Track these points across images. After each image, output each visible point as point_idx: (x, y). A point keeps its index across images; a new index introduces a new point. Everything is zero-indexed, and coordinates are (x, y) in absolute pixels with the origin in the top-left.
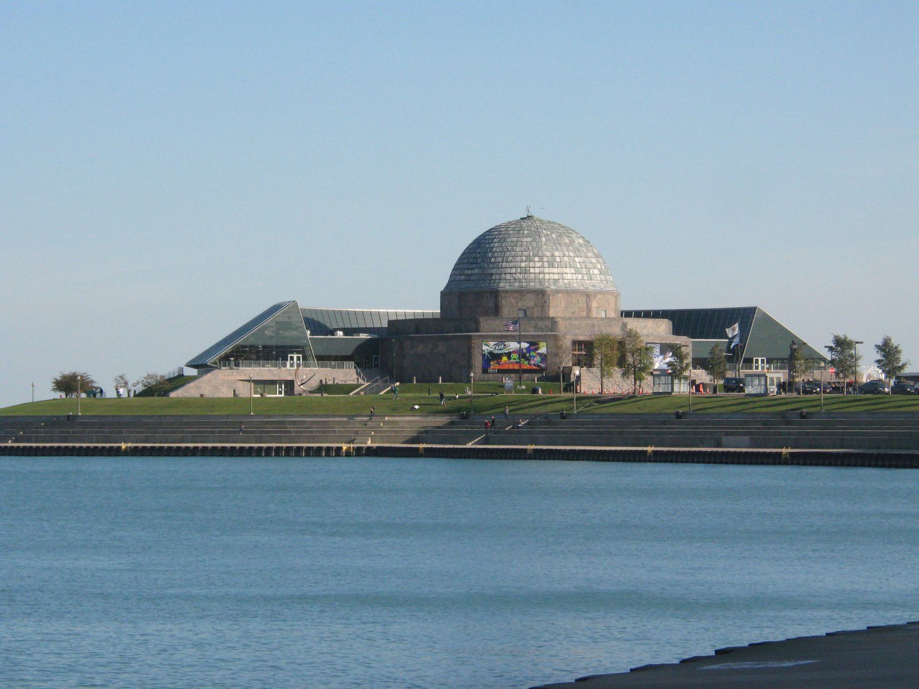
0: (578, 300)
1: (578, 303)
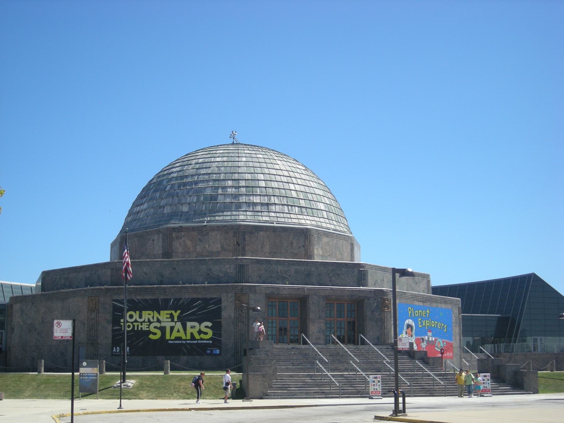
0: (292, 243)
1: (292, 246)
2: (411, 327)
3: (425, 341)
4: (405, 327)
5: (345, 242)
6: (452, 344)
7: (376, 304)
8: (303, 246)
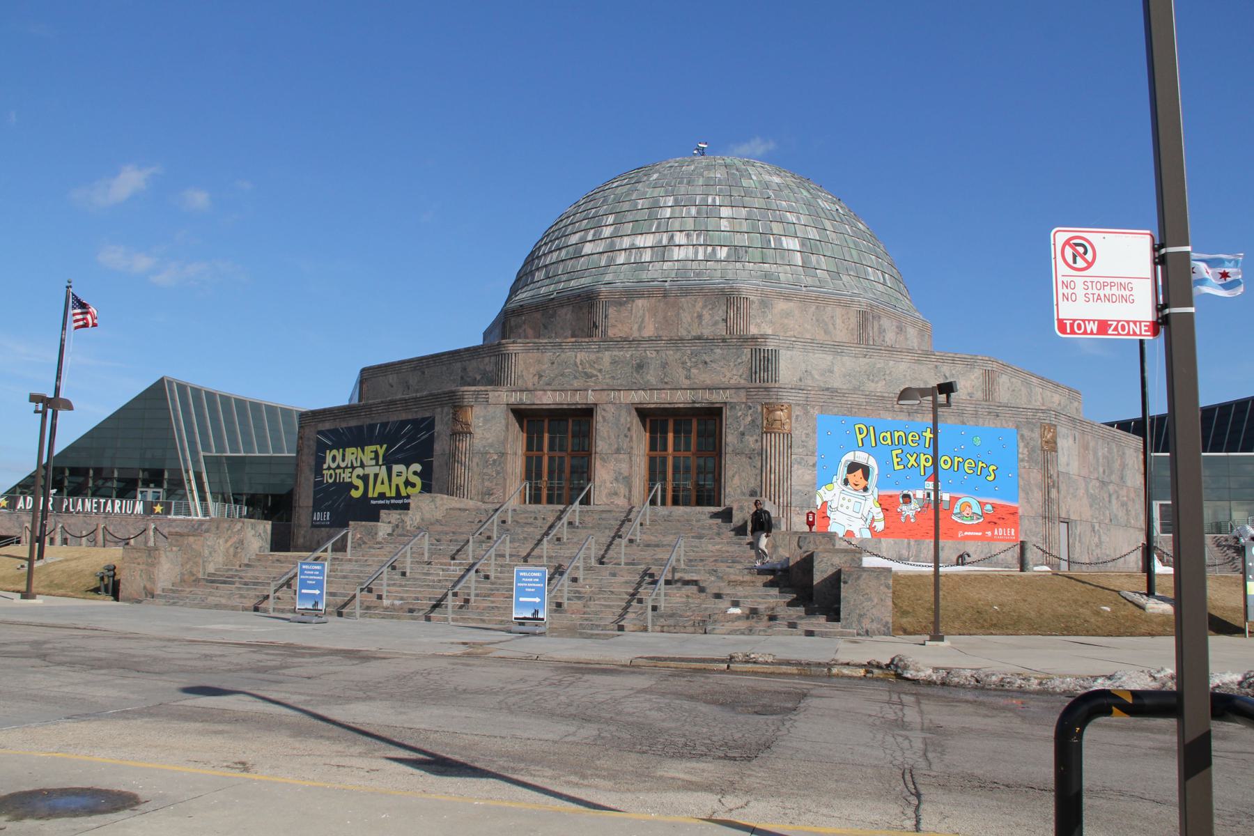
0: (700, 317)
1: (700, 324)
3: (913, 500)
4: (842, 471)
5: (839, 311)
6: (1017, 508)
7: (750, 418)
8: (723, 320)
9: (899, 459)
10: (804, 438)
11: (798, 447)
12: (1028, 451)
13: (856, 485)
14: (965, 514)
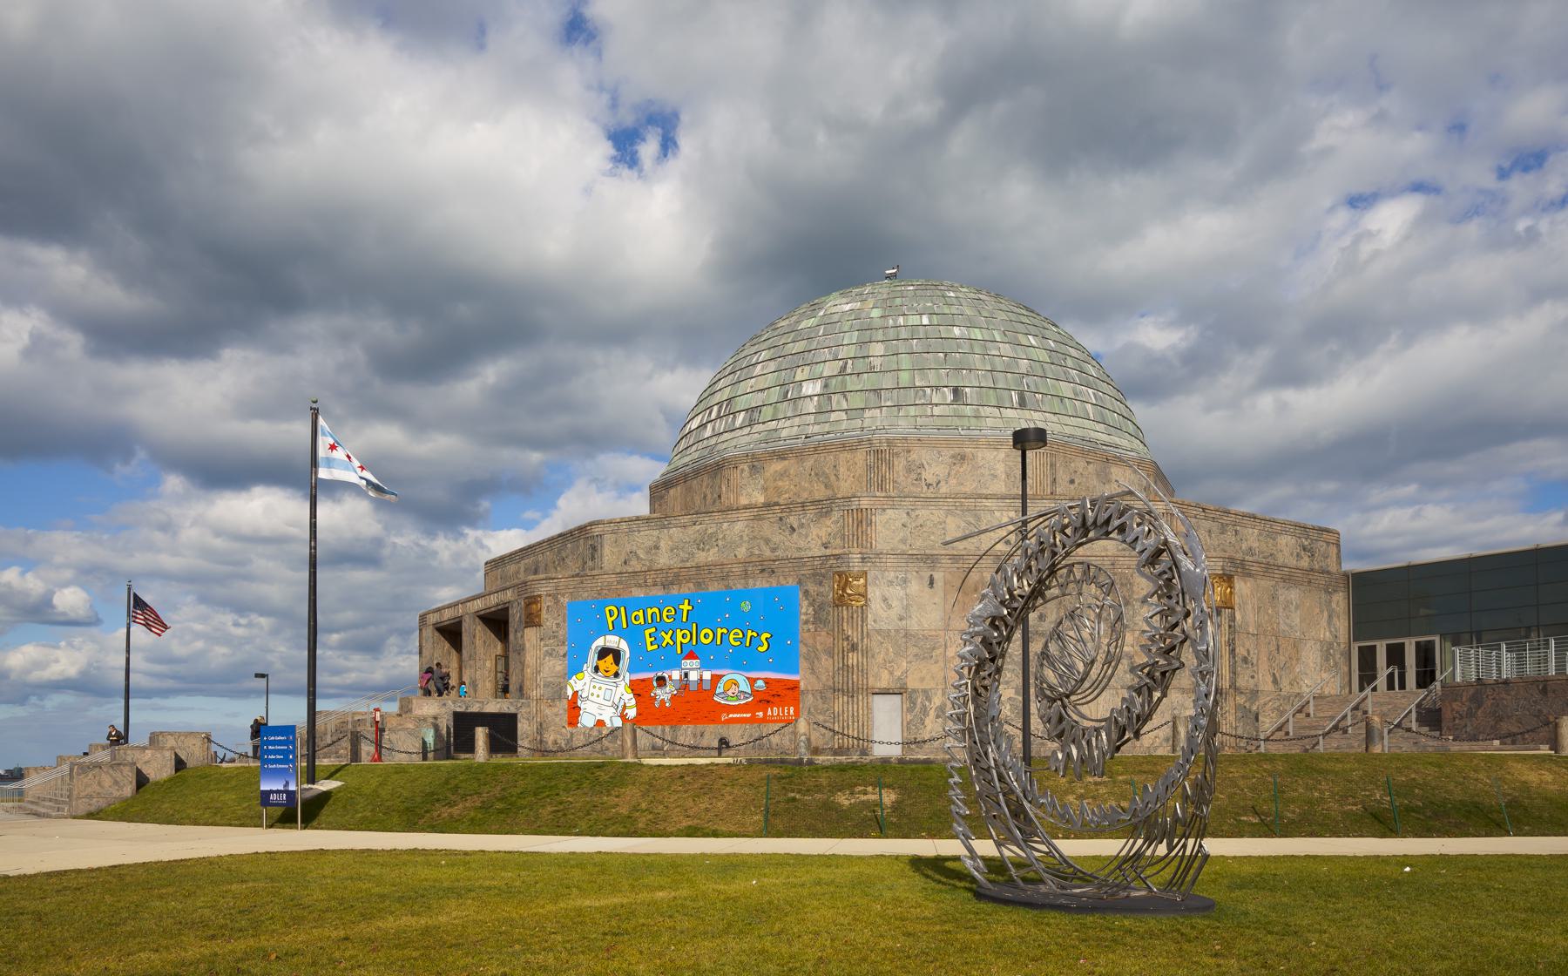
0: (705, 497)
2: (617, 655)
3: (668, 682)
4: (592, 657)
6: (798, 682)
9: (653, 639)
10: (554, 628)
11: (550, 639)
12: (814, 610)
13: (607, 672)
14: (730, 693)
